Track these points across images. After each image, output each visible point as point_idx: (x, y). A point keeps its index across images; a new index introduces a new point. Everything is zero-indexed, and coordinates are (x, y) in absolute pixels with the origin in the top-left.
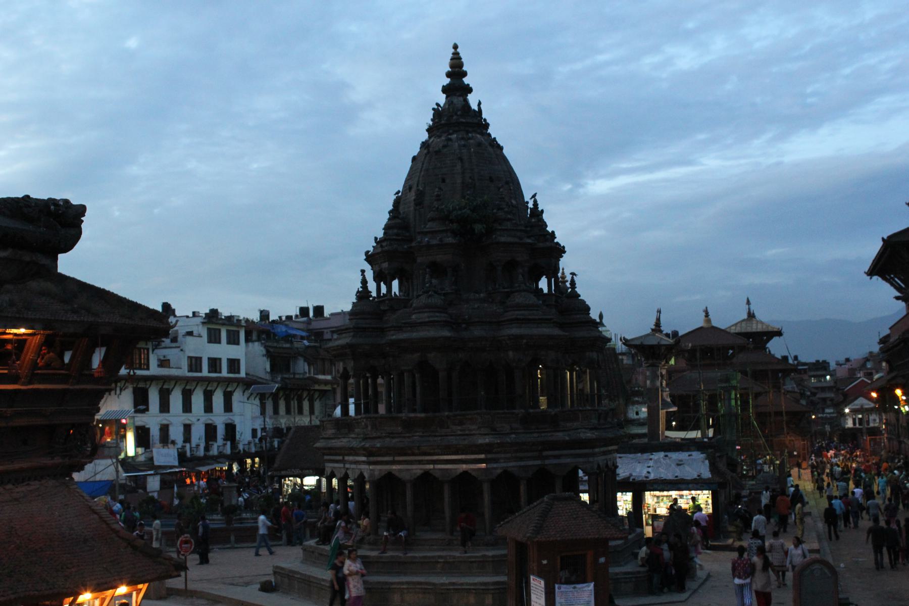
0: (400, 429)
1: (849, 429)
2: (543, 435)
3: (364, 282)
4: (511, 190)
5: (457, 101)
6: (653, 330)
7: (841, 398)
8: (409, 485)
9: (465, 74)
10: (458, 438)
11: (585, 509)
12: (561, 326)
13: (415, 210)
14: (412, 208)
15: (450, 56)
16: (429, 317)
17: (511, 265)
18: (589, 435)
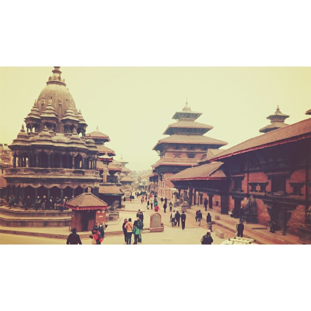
3: (23, 127)
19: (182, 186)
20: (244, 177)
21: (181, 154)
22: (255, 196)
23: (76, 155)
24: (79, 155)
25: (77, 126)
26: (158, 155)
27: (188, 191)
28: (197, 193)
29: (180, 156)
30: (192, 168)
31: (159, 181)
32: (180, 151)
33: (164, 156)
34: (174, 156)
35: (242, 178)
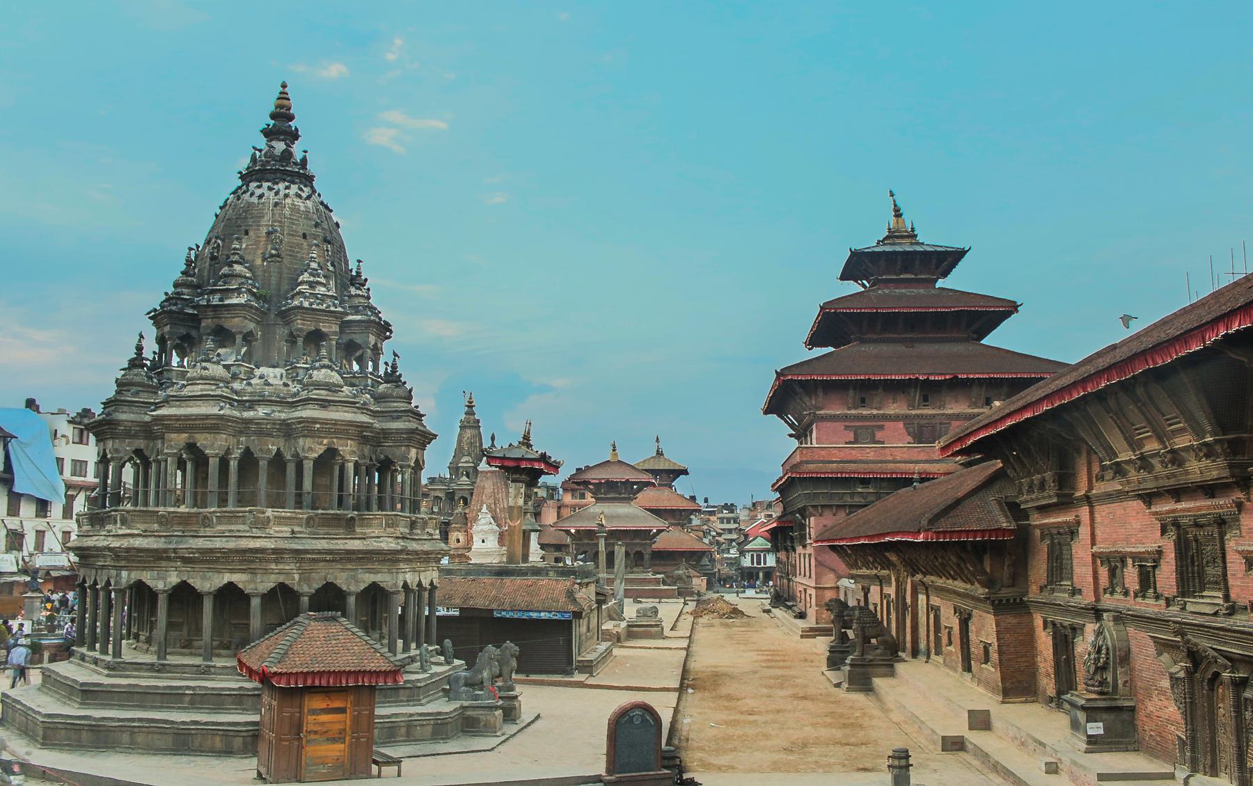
0: (156, 526)
1: (747, 568)
2: (334, 541)
3: (139, 349)
4: (328, 251)
5: (280, 146)
6: (520, 442)
7: (742, 538)
8: (161, 597)
9: (291, 118)
10: (224, 539)
11: (350, 633)
12: (374, 414)
13: (210, 265)
14: (207, 264)
15: (277, 95)
16: (201, 390)
17: (316, 338)
18: (392, 545)
19: (874, 572)
20: (1078, 523)
21: (882, 427)
22: (1120, 618)
23: (320, 450)
24: (331, 453)
25: (334, 333)
26: (791, 436)
27: (891, 591)
28: (922, 598)
29: (879, 435)
30: (915, 488)
31: (799, 549)
32: (875, 412)
33: (809, 439)
34: (851, 436)
35: (1072, 532)
